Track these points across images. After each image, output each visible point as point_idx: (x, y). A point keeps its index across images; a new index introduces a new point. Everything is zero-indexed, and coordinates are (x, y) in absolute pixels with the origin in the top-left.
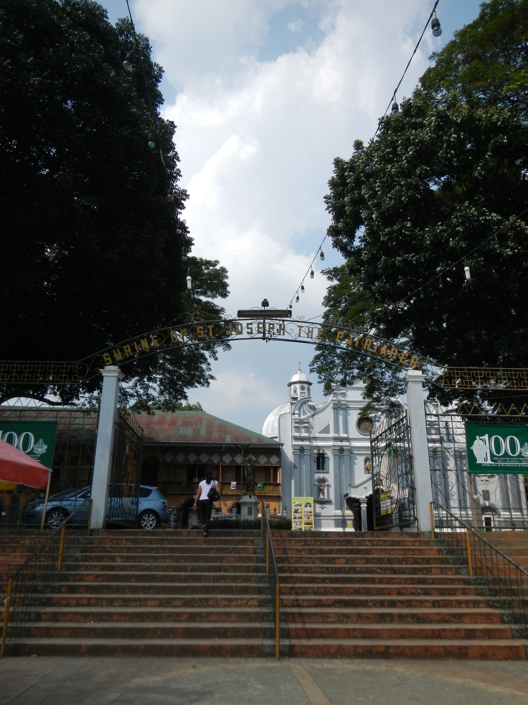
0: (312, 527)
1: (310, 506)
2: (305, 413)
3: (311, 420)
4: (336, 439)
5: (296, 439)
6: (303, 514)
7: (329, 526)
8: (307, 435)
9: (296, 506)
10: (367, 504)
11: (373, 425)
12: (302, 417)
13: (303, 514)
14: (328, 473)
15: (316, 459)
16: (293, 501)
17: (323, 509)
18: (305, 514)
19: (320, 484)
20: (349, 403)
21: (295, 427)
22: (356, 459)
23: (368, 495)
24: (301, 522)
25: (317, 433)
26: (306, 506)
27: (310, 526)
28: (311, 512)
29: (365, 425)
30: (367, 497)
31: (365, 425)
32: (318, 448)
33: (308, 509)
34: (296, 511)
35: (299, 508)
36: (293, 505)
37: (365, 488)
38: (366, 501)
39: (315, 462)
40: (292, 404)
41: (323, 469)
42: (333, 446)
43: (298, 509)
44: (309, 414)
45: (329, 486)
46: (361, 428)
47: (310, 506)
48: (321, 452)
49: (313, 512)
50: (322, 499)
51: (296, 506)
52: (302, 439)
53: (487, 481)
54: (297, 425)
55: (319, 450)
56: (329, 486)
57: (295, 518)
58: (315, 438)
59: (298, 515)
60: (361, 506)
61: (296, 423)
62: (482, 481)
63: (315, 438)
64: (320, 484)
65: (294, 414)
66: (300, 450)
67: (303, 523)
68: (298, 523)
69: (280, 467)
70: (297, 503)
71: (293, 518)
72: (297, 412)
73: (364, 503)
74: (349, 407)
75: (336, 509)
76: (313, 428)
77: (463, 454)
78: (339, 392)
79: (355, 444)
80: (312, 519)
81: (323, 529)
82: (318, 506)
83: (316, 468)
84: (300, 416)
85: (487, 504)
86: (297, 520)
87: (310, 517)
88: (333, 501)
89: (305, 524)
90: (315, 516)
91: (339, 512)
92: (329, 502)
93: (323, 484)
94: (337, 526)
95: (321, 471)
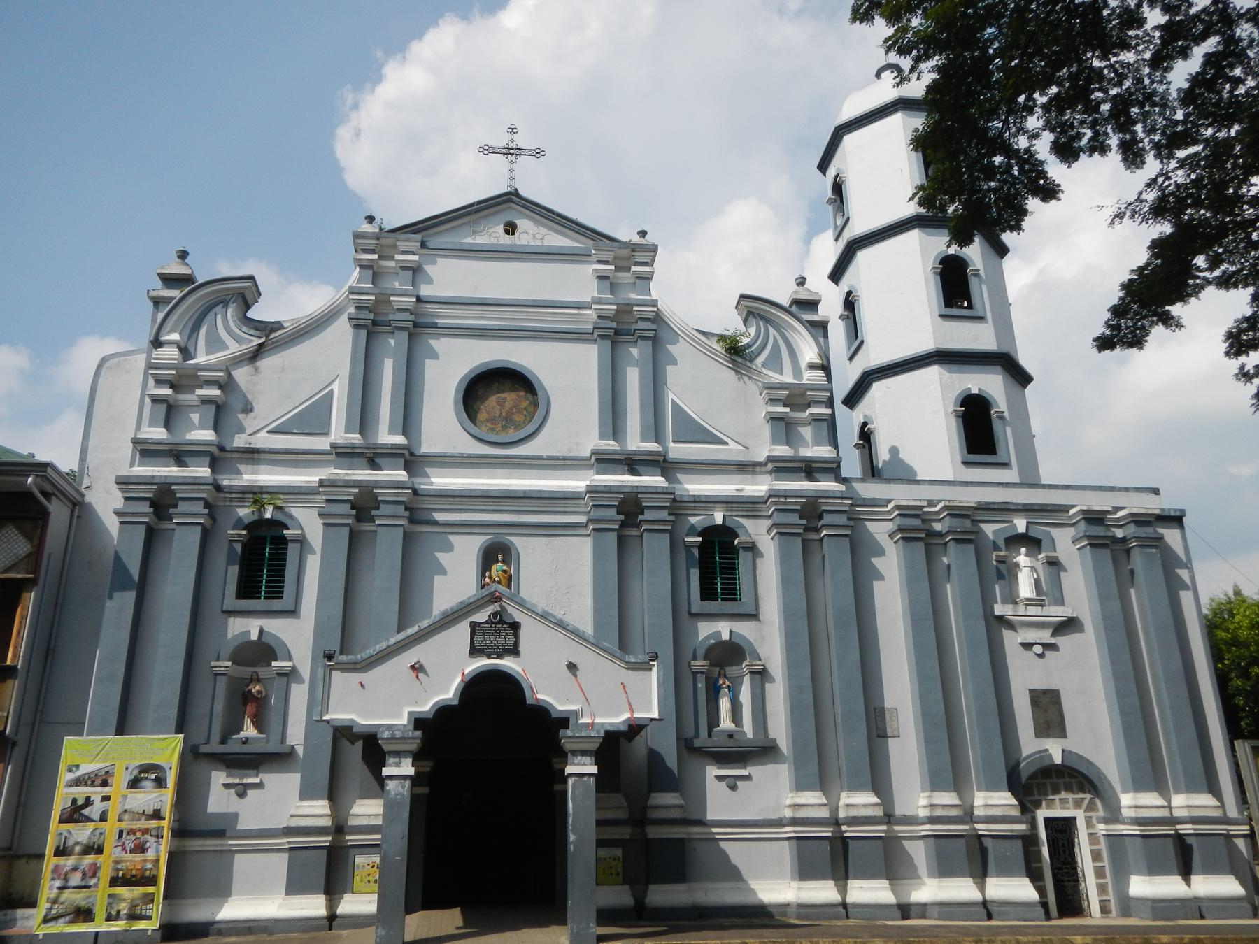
0: (149, 899)
1: (160, 783)
2: (215, 344)
3: (241, 375)
4: (344, 454)
5: (147, 451)
6: (111, 827)
7: (258, 889)
8: (207, 435)
9: (78, 782)
10: (417, 757)
11: (536, 405)
12: (202, 358)
13: (111, 827)
14: (293, 613)
15: (238, 547)
16: (67, 757)
17: (242, 795)
18: (124, 825)
19: (247, 671)
20: (431, 309)
21: (156, 400)
22: (449, 548)
23: (426, 707)
24: (94, 870)
25: (263, 434)
26: (134, 784)
27: (140, 890)
28: (157, 815)
29: (501, 404)
30: (419, 722)
31: (501, 404)
32: (257, 495)
33: (147, 798)
34: (75, 814)
35: (96, 792)
36: (65, 777)
37: (417, 669)
38: (413, 747)
39: (230, 562)
40: (157, 302)
41: (276, 592)
42: (322, 483)
43: (88, 802)
44: (234, 348)
45: (290, 675)
46: (482, 416)
47: (160, 783)
48: (268, 516)
49: (167, 812)
50: (245, 741)
51: (78, 782)
52: (179, 455)
53: (1048, 646)
54: (166, 391)
55: (261, 507)
56: (290, 675)
57: (61, 852)
58: (253, 455)
59: (81, 833)
60: (386, 772)
61: (159, 382)
62: (1027, 646)
63: (253, 455)
64: (247, 671)
65: (157, 343)
66: (154, 504)
67: (105, 874)
68: (75, 879)
69: (31, 583)
70: (86, 768)
71: (50, 848)
72: (175, 336)
73: (398, 754)
74: (435, 326)
75: (306, 794)
76: (248, 409)
77: (938, 527)
78: (392, 264)
79: (441, 480)
80: (159, 850)
81: (234, 910)
82: (219, 778)
83: (232, 588)
84: (185, 352)
85: (1055, 750)
86: (70, 861)
87: (151, 841)
88: (300, 750)
89: (114, 882)
90: (182, 831)
91: (318, 811)
92: (280, 759)
93: (263, 672)
94: (295, 886)
95: (260, 604)
